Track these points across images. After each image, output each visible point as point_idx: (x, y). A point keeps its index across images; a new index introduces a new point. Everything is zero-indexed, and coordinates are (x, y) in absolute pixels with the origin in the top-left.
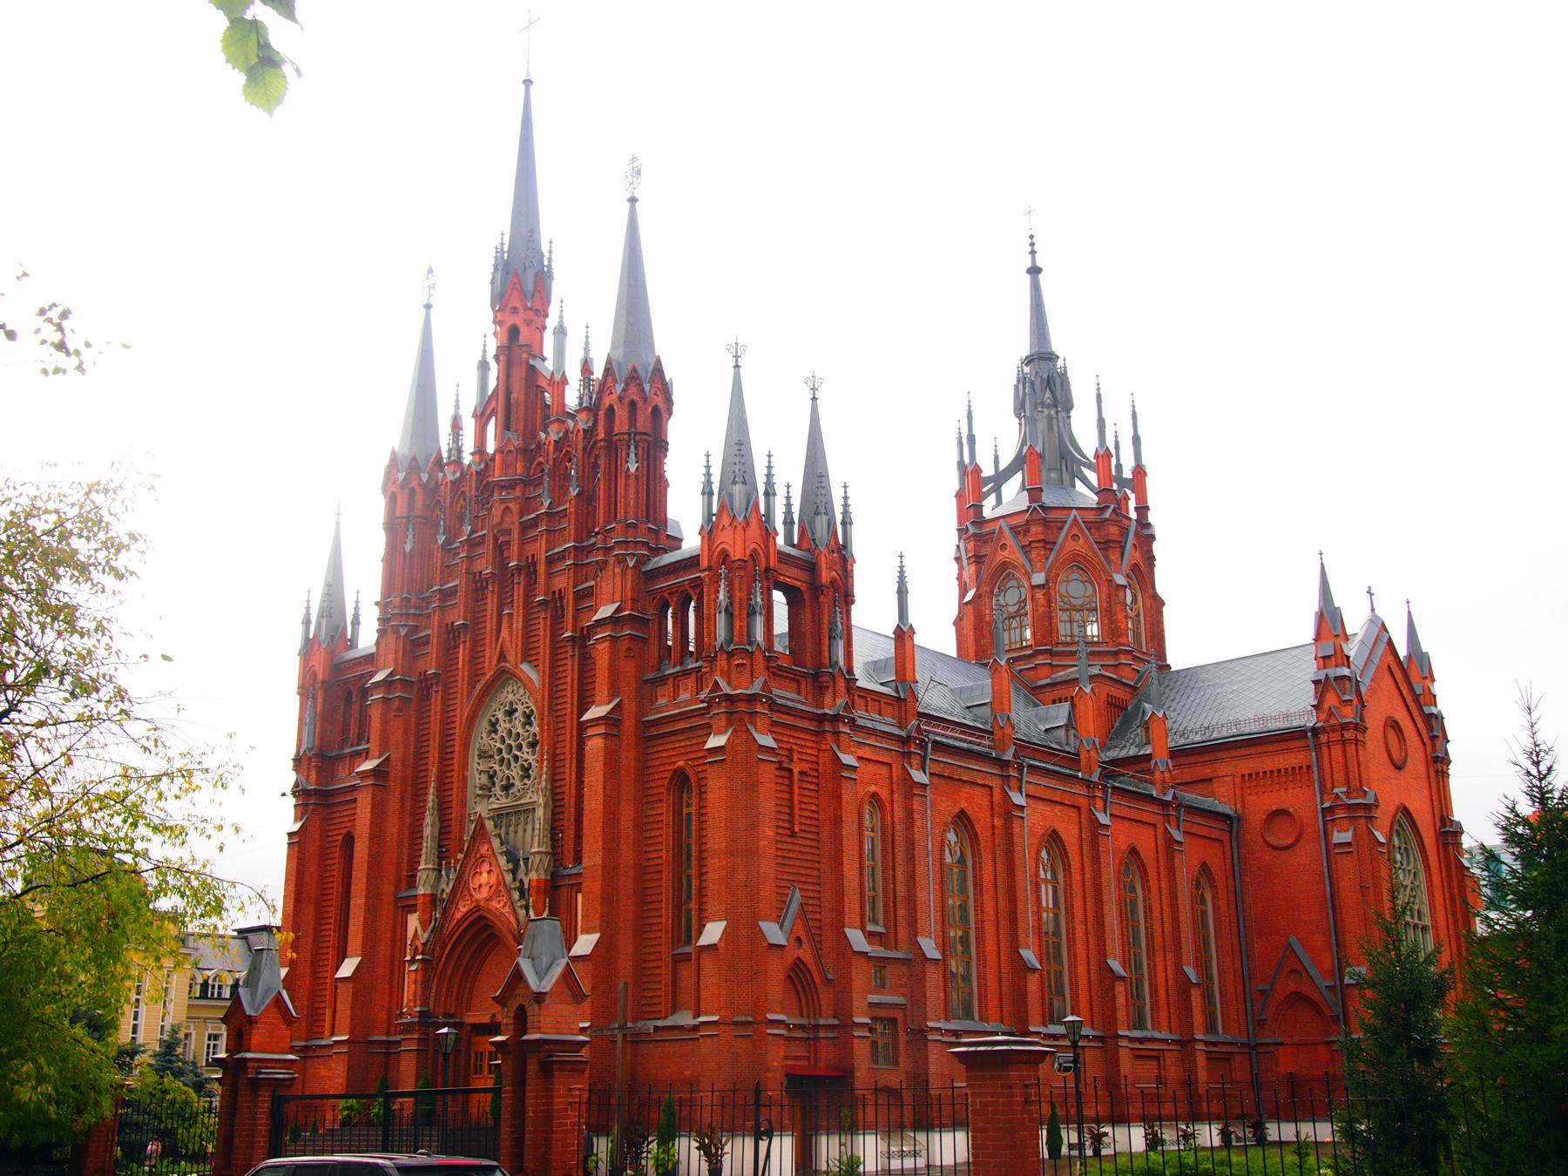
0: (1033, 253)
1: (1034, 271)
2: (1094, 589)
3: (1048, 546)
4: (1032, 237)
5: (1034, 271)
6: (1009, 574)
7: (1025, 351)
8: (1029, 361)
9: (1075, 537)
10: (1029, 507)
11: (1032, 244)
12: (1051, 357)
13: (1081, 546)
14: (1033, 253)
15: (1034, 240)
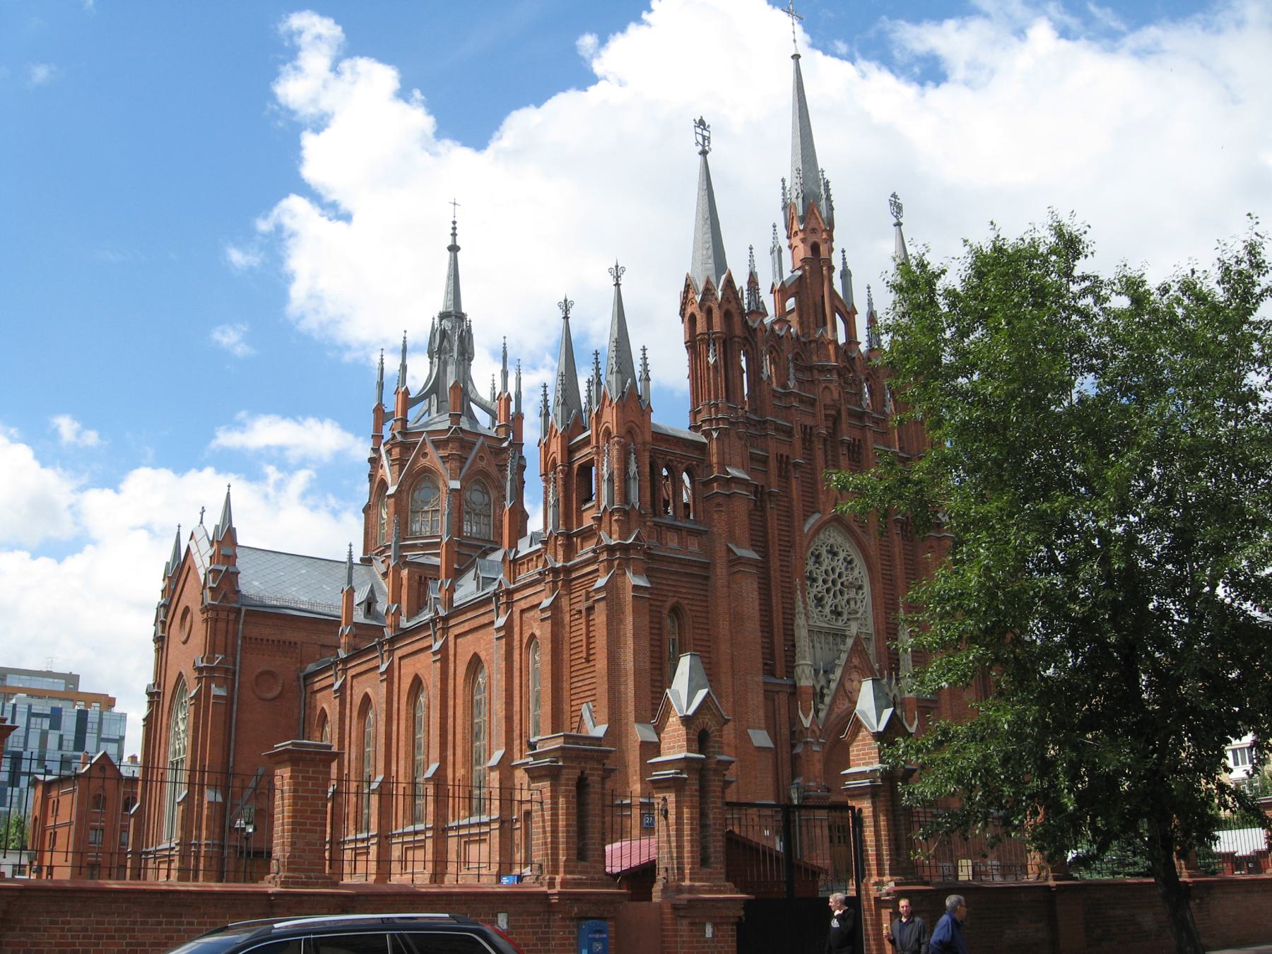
0: (454, 235)
1: (454, 249)
2: (490, 500)
3: (463, 460)
4: (454, 223)
5: (454, 249)
6: (425, 477)
7: (439, 306)
8: (443, 316)
9: (482, 458)
10: (450, 428)
11: (454, 229)
12: (461, 317)
13: (482, 464)
14: (454, 235)
15: (457, 225)
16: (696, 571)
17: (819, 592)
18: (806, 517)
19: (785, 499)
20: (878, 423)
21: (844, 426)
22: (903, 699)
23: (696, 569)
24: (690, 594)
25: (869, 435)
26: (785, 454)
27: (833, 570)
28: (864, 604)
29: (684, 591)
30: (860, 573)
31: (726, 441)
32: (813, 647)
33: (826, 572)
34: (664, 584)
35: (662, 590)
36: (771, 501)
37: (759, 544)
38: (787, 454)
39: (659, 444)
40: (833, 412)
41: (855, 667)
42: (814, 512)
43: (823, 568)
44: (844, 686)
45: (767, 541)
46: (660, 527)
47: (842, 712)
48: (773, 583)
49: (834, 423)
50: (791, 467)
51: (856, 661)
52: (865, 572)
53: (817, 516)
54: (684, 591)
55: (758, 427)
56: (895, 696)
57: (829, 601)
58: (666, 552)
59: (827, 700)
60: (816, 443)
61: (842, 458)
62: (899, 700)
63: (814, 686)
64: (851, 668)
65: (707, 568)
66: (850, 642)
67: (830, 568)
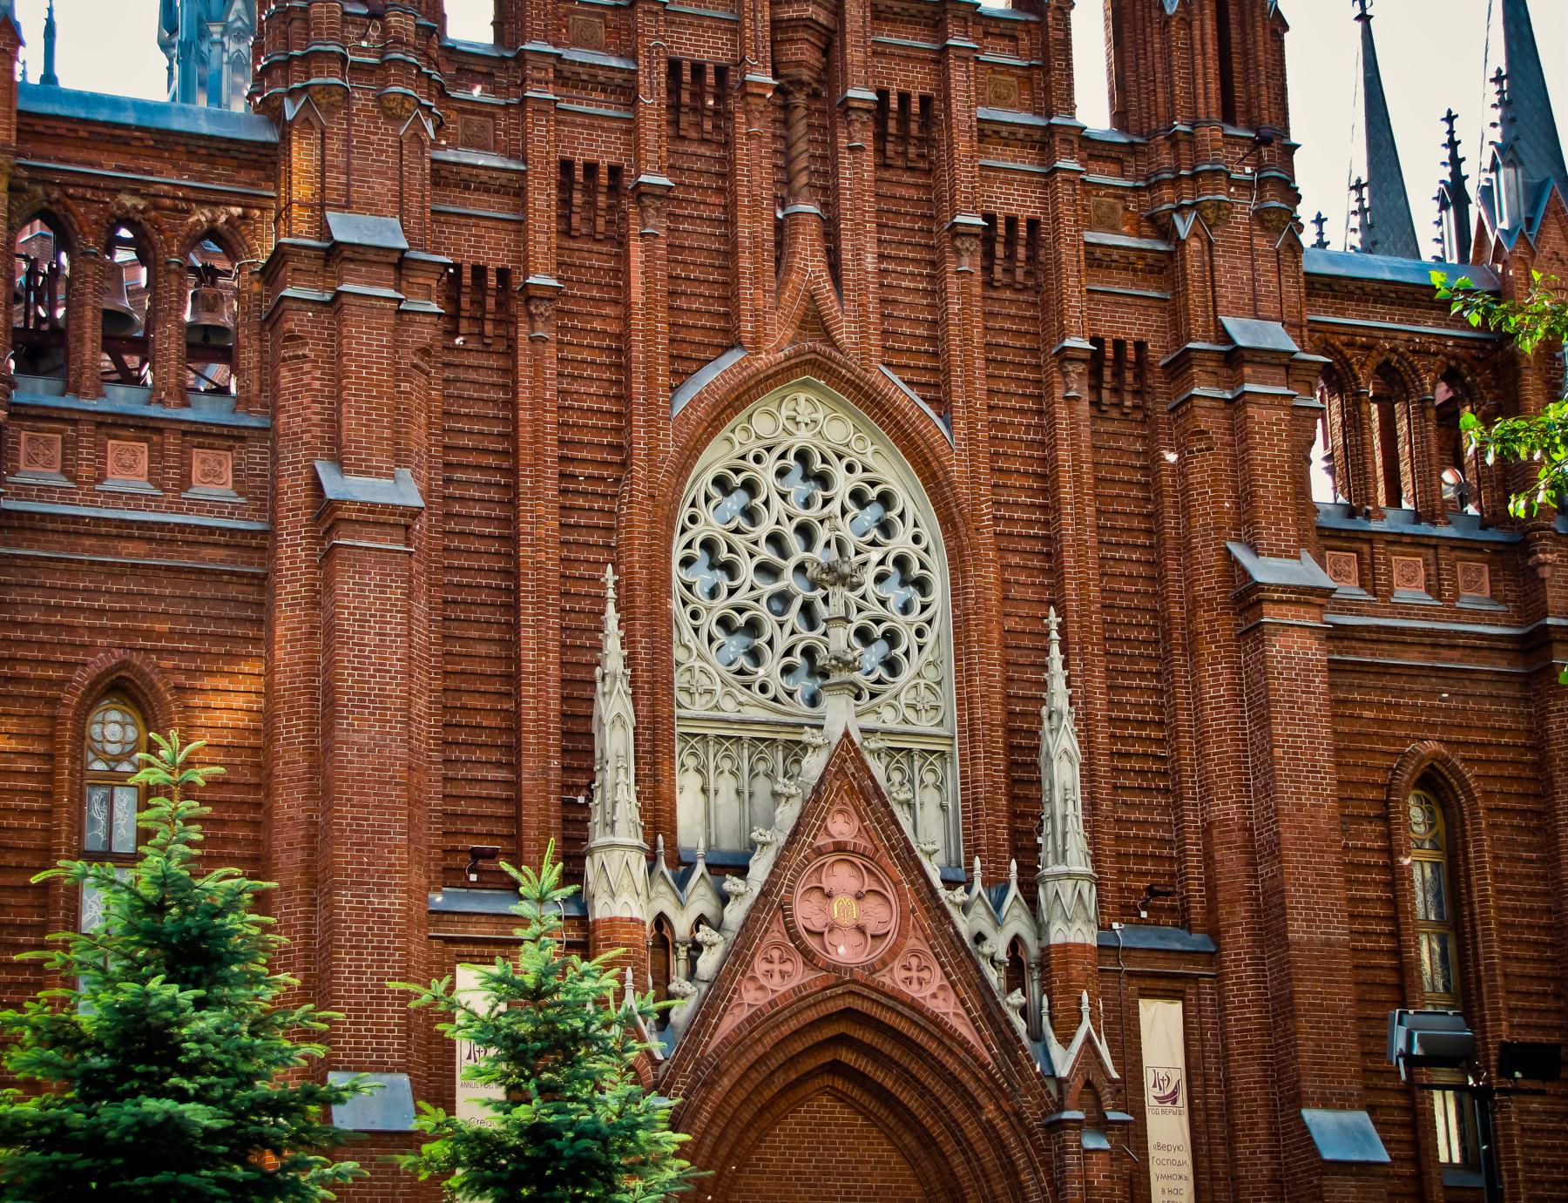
16: (213, 558)
17: (740, 611)
18: (683, 368)
19: (608, 311)
20: (1014, 38)
21: (854, 55)
22: (1046, 951)
23: (222, 553)
24: (184, 636)
25: (958, 75)
26: (604, 162)
27: (805, 531)
28: (930, 637)
29: (164, 627)
30: (916, 539)
31: (337, 127)
32: (704, 790)
33: (775, 540)
34: (79, 609)
35: (71, 628)
36: (531, 316)
37: (491, 461)
38: (613, 160)
39: (93, 156)
40: (823, 17)
41: (840, 847)
42: (726, 349)
43: (766, 527)
44: (784, 909)
45: (514, 454)
46: (74, 422)
47: (772, 1003)
48: (527, 585)
49: (826, 51)
50: (627, 204)
51: (842, 827)
52: (931, 530)
53: (731, 359)
54: (164, 627)
55: (502, 79)
56: (1016, 943)
57: (784, 632)
58: (93, 504)
59: (708, 963)
60: (741, 118)
61: (846, 160)
62: (1032, 949)
63: (661, 921)
64: (819, 852)
65: (261, 548)
66: (814, 765)
67: (788, 530)
